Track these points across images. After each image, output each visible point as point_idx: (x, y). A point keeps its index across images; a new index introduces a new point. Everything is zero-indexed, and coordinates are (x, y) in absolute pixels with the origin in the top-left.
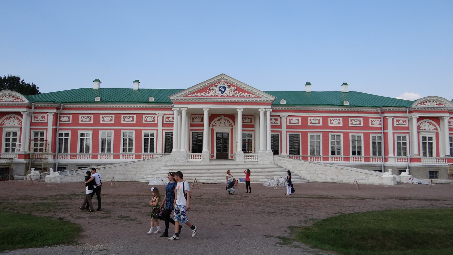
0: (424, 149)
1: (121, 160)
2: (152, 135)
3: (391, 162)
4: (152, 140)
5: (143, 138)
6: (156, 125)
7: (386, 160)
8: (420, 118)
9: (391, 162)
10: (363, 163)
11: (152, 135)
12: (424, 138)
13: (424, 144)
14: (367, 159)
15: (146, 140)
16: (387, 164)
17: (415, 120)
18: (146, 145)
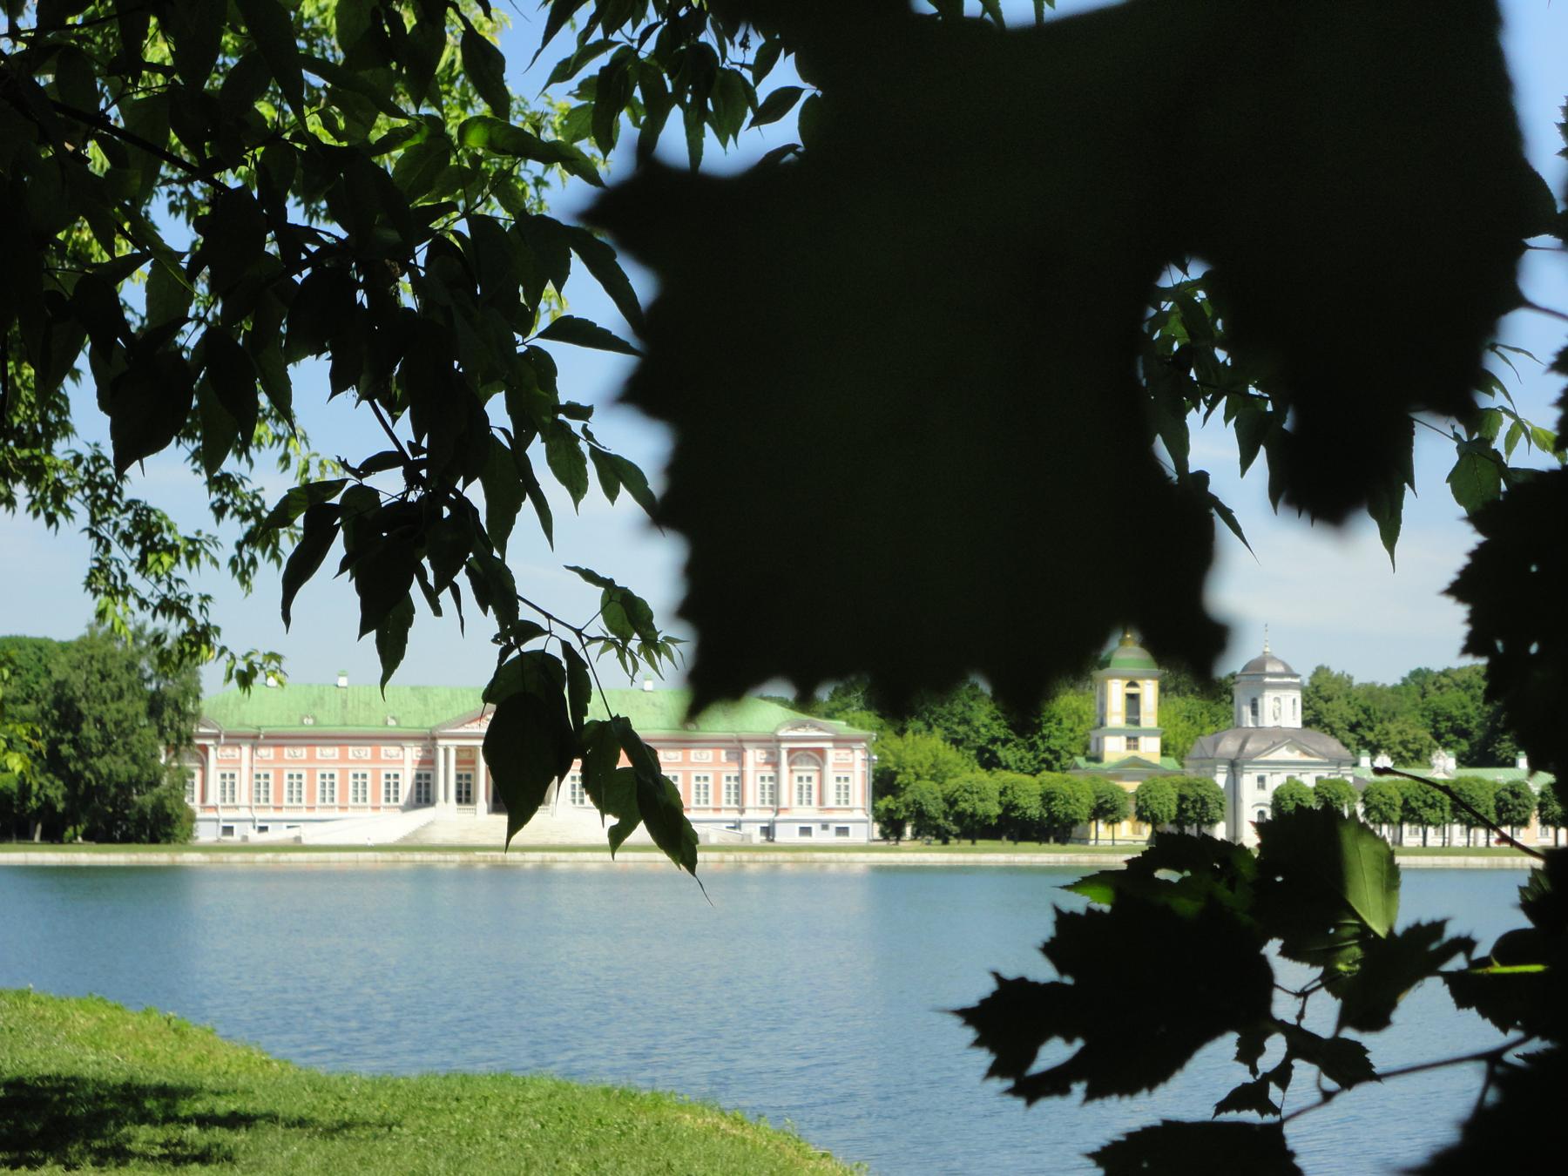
0: (801, 795)
1: (350, 813)
2: (396, 776)
3: (749, 815)
4: (397, 785)
5: (383, 781)
6: (402, 762)
7: (742, 811)
8: (791, 751)
9: (749, 815)
10: (711, 815)
11: (396, 776)
12: (800, 779)
13: (801, 787)
14: (717, 810)
15: (388, 785)
16: (744, 817)
17: (784, 754)
18: (388, 792)
